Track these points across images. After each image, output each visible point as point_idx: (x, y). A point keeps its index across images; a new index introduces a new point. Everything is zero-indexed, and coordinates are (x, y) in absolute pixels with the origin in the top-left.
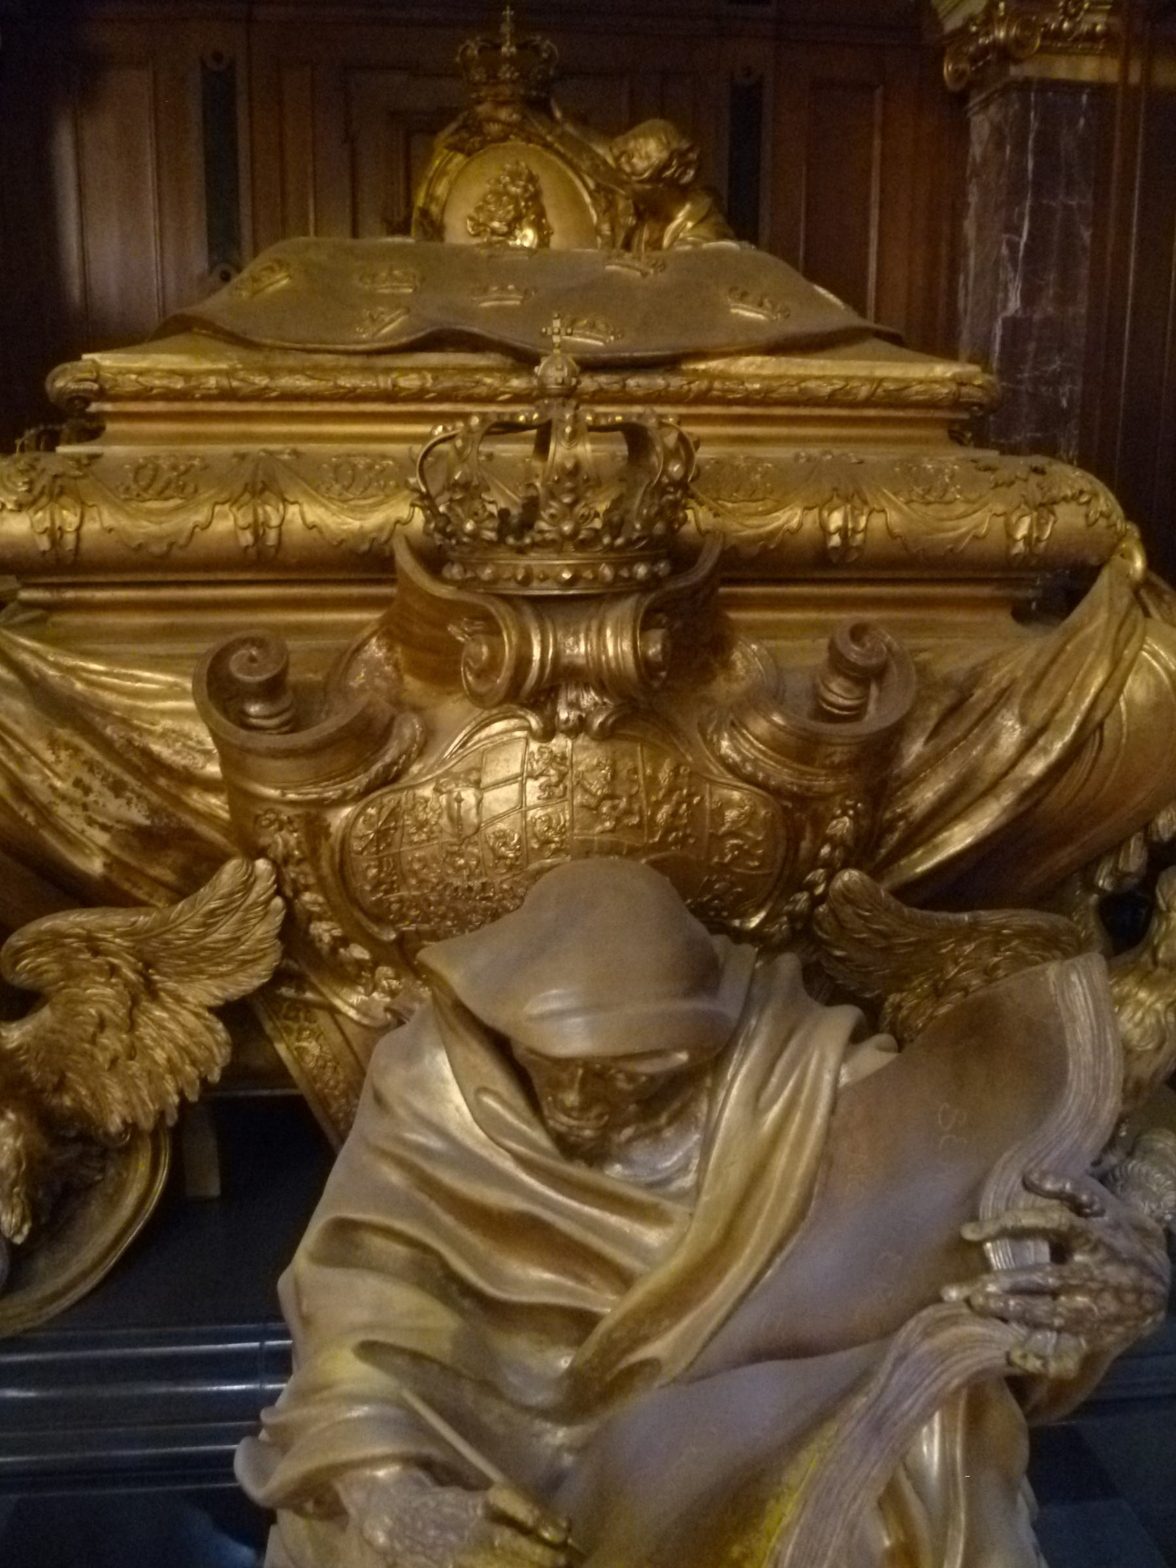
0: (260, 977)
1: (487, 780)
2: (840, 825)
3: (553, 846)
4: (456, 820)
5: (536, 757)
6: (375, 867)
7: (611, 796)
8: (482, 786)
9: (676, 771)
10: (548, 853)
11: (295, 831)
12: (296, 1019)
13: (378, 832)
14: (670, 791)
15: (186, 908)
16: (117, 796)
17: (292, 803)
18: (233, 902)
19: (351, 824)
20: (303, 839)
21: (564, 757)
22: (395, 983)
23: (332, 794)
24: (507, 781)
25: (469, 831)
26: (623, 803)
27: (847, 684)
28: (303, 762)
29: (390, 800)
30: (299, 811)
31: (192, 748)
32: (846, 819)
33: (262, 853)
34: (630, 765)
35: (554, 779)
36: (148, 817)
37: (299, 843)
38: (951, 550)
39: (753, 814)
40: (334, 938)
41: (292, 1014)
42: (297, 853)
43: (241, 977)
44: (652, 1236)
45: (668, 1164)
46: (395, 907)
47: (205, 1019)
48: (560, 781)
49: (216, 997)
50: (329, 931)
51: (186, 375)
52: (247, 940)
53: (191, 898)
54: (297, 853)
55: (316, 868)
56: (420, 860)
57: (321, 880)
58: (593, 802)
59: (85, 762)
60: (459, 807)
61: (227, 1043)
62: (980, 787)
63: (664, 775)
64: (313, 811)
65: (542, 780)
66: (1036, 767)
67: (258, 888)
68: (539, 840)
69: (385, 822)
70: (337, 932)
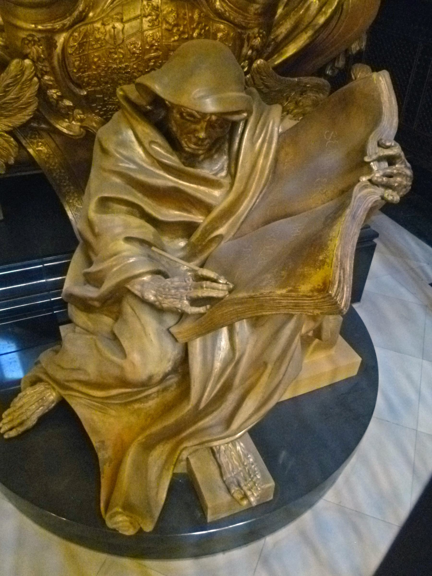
0: (28, 115)
1: (125, 19)
2: (257, 41)
3: (154, 47)
4: (114, 37)
5: (147, 7)
6: (78, 60)
7: (177, 25)
9: (199, 15)
10: (152, 51)
11: (41, 45)
12: (35, 138)
13: (79, 44)
14: (198, 23)
17: (40, 31)
18: (17, 80)
19: (66, 41)
20: (45, 49)
21: (158, 7)
22: (82, 116)
23: (58, 26)
24: (135, 18)
25: (120, 42)
26: (181, 29)
28: (44, 10)
29: (83, 29)
30: (44, 35)
32: (259, 38)
33: (26, 56)
34: (183, 12)
35: (154, 17)
37: (43, 51)
39: (228, 34)
40: (58, 96)
41: (33, 136)
42: (42, 56)
43: (19, 116)
44: (217, 193)
45: (217, 168)
46: (86, 80)
47: (5, 137)
49: (9, 126)
50: (55, 93)
52: (22, 99)
54: (42, 56)
55: (51, 63)
56: (97, 57)
57: (53, 68)
58: (170, 28)
60: (114, 31)
61: (15, 146)
62: (302, 27)
63: (196, 16)
64: (50, 35)
65: (149, 18)
66: (322, 20)
67: (27, 73)
68: (149, 45)
69: (83, 39)
70: (59, 94)
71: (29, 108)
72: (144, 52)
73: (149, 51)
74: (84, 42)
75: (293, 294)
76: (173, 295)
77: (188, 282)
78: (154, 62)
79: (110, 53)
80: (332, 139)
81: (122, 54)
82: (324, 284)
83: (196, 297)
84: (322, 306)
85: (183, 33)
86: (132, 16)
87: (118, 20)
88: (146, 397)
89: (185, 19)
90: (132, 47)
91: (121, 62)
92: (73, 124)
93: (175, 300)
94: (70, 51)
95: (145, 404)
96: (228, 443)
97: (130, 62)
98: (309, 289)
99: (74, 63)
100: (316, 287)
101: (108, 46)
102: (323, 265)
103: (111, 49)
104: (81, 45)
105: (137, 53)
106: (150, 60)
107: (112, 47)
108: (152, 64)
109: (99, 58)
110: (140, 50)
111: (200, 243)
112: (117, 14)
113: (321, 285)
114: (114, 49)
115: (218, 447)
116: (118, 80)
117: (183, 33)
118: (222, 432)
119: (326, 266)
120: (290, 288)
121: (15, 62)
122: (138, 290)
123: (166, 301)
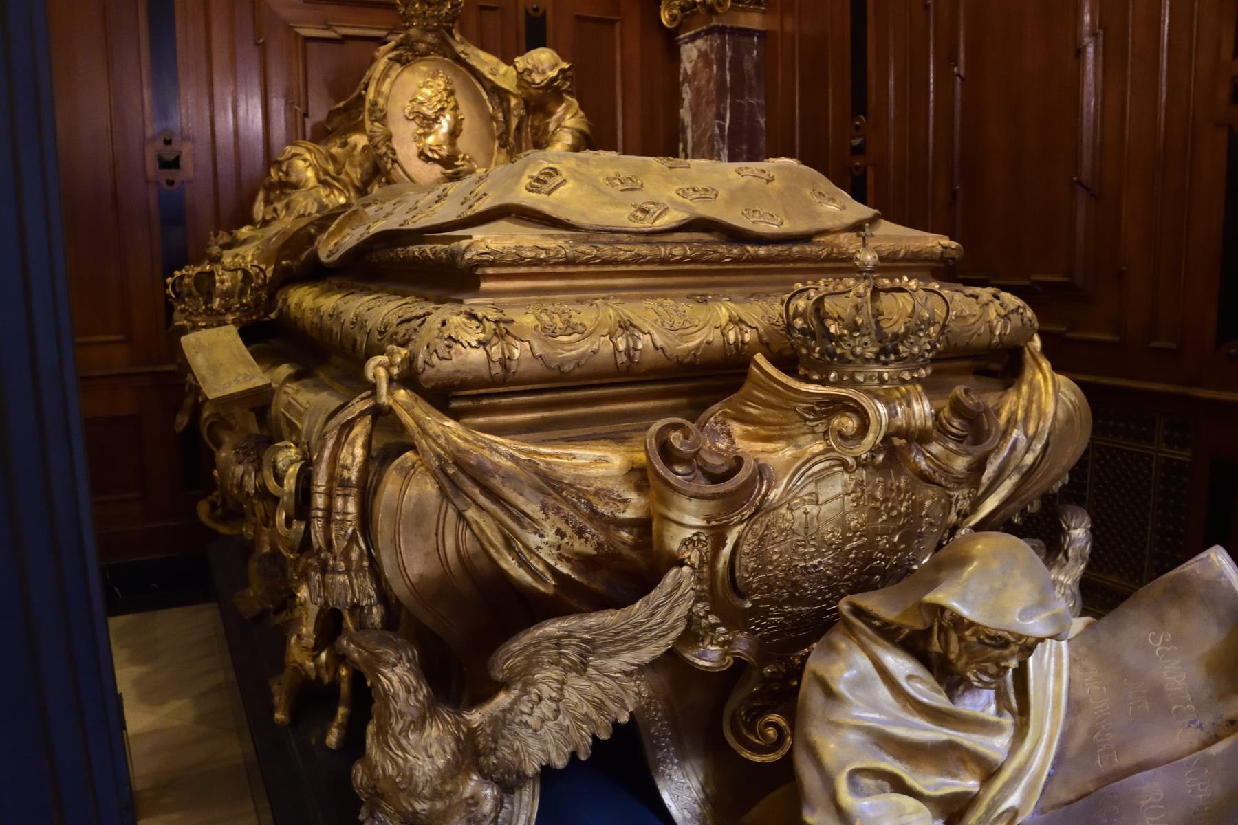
1: (821, 500)
6: (754, 561)
7: (886, 500)
8: (819, 503)
15: (643, 605)
16: (580, 537)
17: (713, 527)
26: (890, 504)
27: (965, 423)
29: (766, 520)
31: (614, 500)
33: (681, 563)
35: (860, 494)
36: (595, 549)
38: (968, 343)
45: (982, 702)
46: (755, 585)
48: (862, 495)
50: (703, 608)
51: (547, 250)
53: (646, 598)
59: (563, 517)
65: (853, 495)
66: (1029, 459)
69: (764, 532)
70: (707, 608)
71: (670, 635)
73: (850, 540)
74: (766, 535)
78: (855, 553)
79: (798, 546)
80: (1164, 643)
81: (813, 546)
85: (893, 508)
86: (831, 495)
87: (811, 502)
89: (892, 491)
91: (812, 558)
92: (709, 650)
94: (746, 549)
97: (824, 557)
99: (747, 567)
101: (796, 538)
103: (799, 541)
104: (761, 539)
106: (850, 551)
107: (799, 538)
108: (853, 556)
109: (781, 553)
112: (810, 494)
116: (804, 582)
117: (893, 508)
121: (673, 571)
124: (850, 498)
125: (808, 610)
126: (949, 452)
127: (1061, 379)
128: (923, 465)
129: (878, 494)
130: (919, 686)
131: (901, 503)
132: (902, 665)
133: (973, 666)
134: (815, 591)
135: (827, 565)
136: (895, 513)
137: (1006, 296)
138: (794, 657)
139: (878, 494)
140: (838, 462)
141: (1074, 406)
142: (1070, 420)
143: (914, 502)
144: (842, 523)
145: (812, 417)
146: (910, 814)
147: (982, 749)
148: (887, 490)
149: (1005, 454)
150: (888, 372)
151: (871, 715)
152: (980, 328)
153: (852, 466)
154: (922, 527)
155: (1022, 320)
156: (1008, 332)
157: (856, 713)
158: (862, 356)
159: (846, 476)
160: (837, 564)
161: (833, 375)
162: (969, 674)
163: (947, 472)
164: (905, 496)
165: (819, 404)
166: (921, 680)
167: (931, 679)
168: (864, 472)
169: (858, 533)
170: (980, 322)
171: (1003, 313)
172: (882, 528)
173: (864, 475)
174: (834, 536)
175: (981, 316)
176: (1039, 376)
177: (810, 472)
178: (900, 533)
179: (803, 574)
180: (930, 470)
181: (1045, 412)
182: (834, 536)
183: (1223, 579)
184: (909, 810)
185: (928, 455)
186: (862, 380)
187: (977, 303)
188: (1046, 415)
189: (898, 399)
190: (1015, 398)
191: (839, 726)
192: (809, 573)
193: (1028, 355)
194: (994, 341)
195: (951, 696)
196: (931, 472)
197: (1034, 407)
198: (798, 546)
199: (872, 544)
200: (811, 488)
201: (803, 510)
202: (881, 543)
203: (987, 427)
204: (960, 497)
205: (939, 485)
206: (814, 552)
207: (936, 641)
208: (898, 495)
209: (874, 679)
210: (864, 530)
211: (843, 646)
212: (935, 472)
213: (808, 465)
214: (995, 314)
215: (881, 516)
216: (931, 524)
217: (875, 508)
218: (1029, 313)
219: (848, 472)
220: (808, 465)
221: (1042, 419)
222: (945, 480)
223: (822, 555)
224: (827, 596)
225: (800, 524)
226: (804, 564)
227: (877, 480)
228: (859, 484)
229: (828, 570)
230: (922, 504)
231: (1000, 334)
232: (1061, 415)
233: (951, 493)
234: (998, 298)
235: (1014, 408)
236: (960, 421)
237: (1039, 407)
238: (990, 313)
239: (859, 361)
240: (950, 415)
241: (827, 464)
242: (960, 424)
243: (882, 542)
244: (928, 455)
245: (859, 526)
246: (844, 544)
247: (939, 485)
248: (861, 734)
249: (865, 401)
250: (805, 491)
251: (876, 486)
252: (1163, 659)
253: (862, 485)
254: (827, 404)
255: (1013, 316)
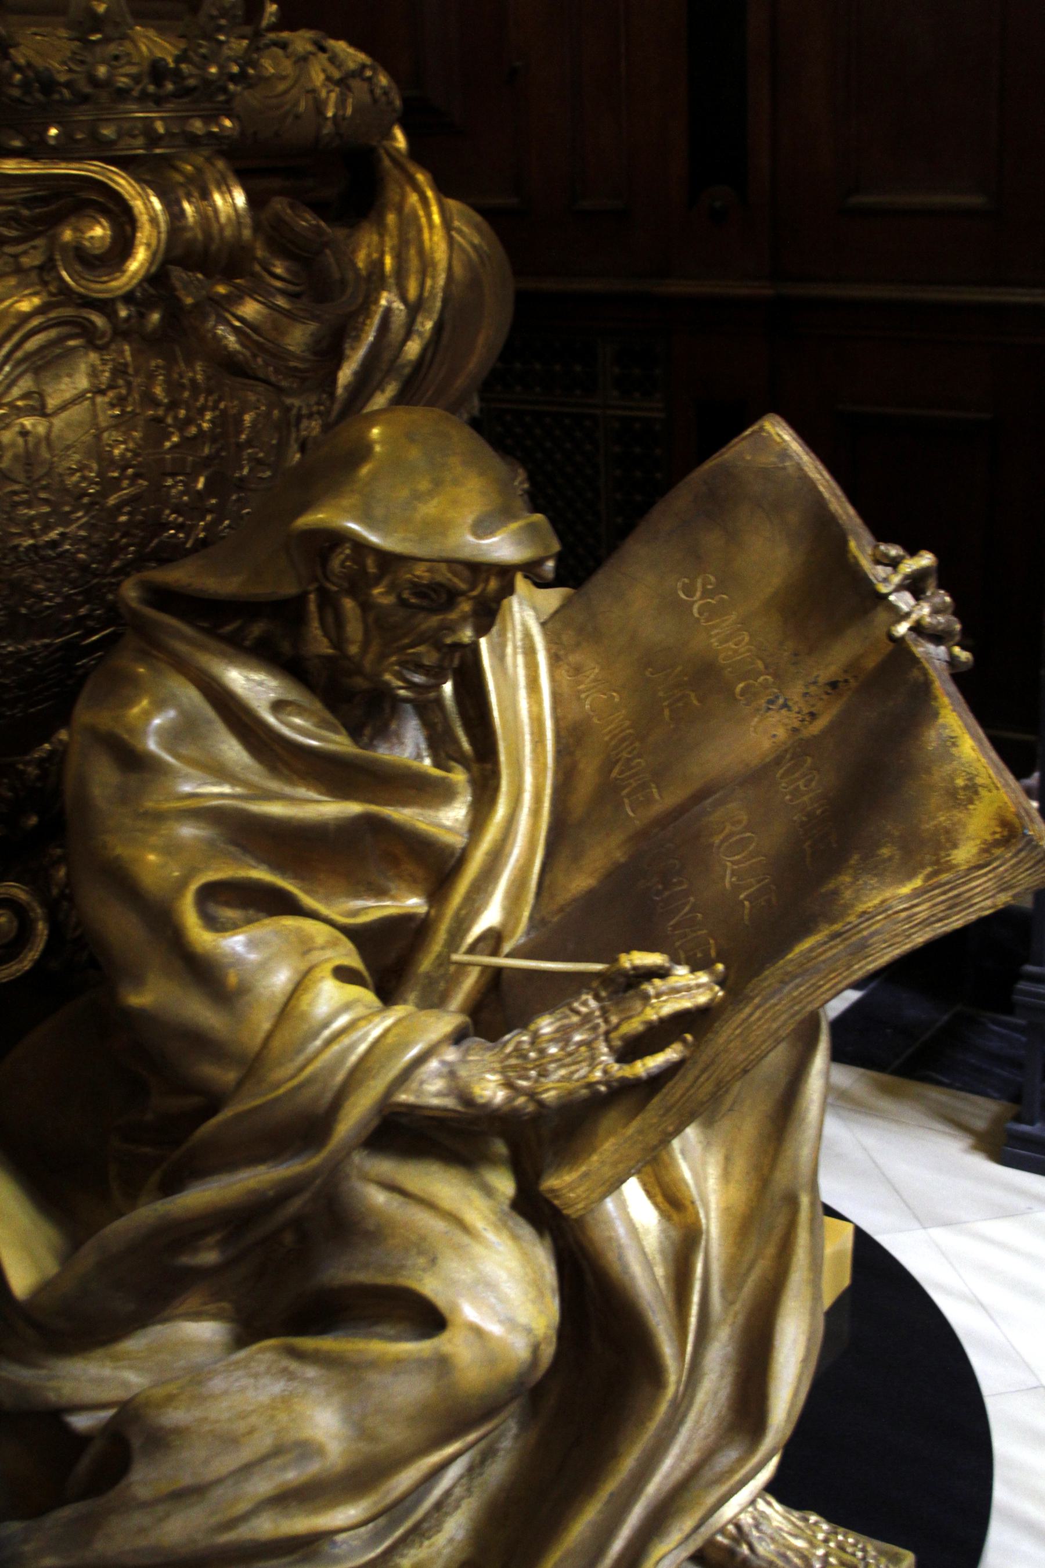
1: (52, 403)
7: (173, 405)
25: (40, 471)
26: (182, 413)
39: (268, 414)
65: (111, 394)
66: (413, 348)
72: (110, 486)
73: (114, 485)
75: (944, 877)
76: (559, 1060)
77: (584, 1010)
78: (129, 513)
80: (705, 593)
81: (46, 501)
82: (1004, 823)
83: (641, 1028)
84: (1014, 878)
87: (30, 411)
88: (438, 1506)
89: (183, 387)
90: (76, 478)
91: (47, 528)
93: (573, 1068)
95: (433, 1540)
96: (753, 1502)
98: (974, 850)
100: (989, 838)
102: (976, 793)
105: (90, 495)
106: (118, 508)
107: (16, 487)
108: (123, 518)
110: (97, 483)
111: (442, 971)
112: (25, 396)
113: (998, 829)
114: (26, 492)
115: (731, 1528)
117: (188, 421)
118: (741, 1461)
119: (983, 792)
120: (929, 869)
122: (439, 1094)
123: (548, 1082)
124: (107, 399)
125: (46, 646)
126: (276, 315)
127: (452, 204)
128: (232, 341)
129: (158, 391)
130: (298, 721)
131: (201, 411)
132: (261, 683)
133: (394, 659)
134: (58, 600)
135: (77, 540)
136: (193, 430)
137: (341, 46)
138: (27, 763)
139: (158, 391)
140: (77, 330)
141: (480, 256)
142: (474, 283)
143: (224, 413)
144: (98, 451)
145: (13, 233)
146: (323, 948)
147: (422, 826)
148: (173, 387)
149: (371, 338)
150: (162, 118)
151: (216, 789)
152: (296, 104)
153: (103, 335)
154: (242, 468)
155: (372, 92)
156: (349, 111)
157: (187, 788)
158: (106, 84)
159: (93, 357)
160: (96, 537)
161: (53, 132)
162: (387, 677)
163: (277, 355)
164: (206, 400)
165: (28, 202)
166: (301, 711)
167: (318, 705)
168: (127, 348)
169: (130, 471)
170: (294, 91)
171: (337, 75)
172: (173, 459)
173: (128, 353)
174: (84, 478)
175: (296, 81)
176: (414, 198)
177: (19, 354)
178: (206, 473)
179: (33, 565)
180: (244, 351)
181: (433, 258)
182: (84, 478)
183: (787, 464)
184: (320, 940)
185: (237, 324)
186: (113, 137)
187: (287, 57)
188: (434, 265)
189: (182, 185)
190: (375, 238)
191: (159, 817)
192: (44, 559)
193: (387, 163)
194: (325, 131)
195: (355, 733)
196: (248, 354)
197: (413, 252)
198: (15, 505)
199: (157, 490)
200: (26, 384)
201: (17, 429)
202: (174, 491)
203: (337, 275)
204: (304, 411)
205: (266, 382)
206: (48, 515)
207: (318, 632)
208: (195, 396)
209: (209, 722)
210: (140, 465)
211: (142, 670)
212: (255, 356)
213: (16, 338)
214: (322, 77)
215: (169, 439)
216: (259, 462)
217: (158, 420)
218: (383, 80)
219: (98, 349)
220: (16, 338)
221: (430, 269)
222: (277, 371)
223: (65, 519)
224: (83, 611)
225: (16, 458)
226: (31, 542)
227: (153, 363)
228: (120, 371)
229: (79, 551)
230: (238, 421)
231: (335, 116)
232: (458, 270)
233: (289, 401)
234: (323, 49)
235: (375, 256)
236: (286, 264)
237: (421, 252)
238: (313, 74)
239: (104, 96)
240: (267, 255)
241: (53, 333)
242: (288, 270)
243: (174, 486)
244: (237, 324)
245: (129, 454)
246: (104, 494)
247: (266, 382)
248: (202, 825)
249: (123, 183)
250: (16, 392)
251: (151, 377)
252: (708, 620)
253: (125, 373)
254: (44, 201)
255: (356, 83)
